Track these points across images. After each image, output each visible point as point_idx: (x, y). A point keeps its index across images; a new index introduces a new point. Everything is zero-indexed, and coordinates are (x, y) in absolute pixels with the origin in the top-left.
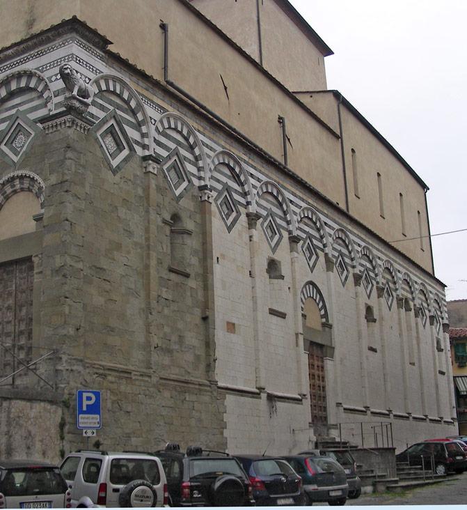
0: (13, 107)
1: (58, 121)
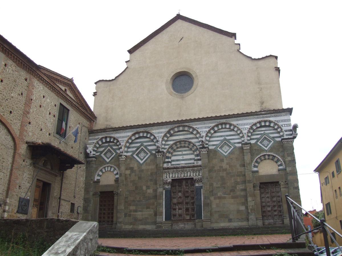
1: (290, 140)
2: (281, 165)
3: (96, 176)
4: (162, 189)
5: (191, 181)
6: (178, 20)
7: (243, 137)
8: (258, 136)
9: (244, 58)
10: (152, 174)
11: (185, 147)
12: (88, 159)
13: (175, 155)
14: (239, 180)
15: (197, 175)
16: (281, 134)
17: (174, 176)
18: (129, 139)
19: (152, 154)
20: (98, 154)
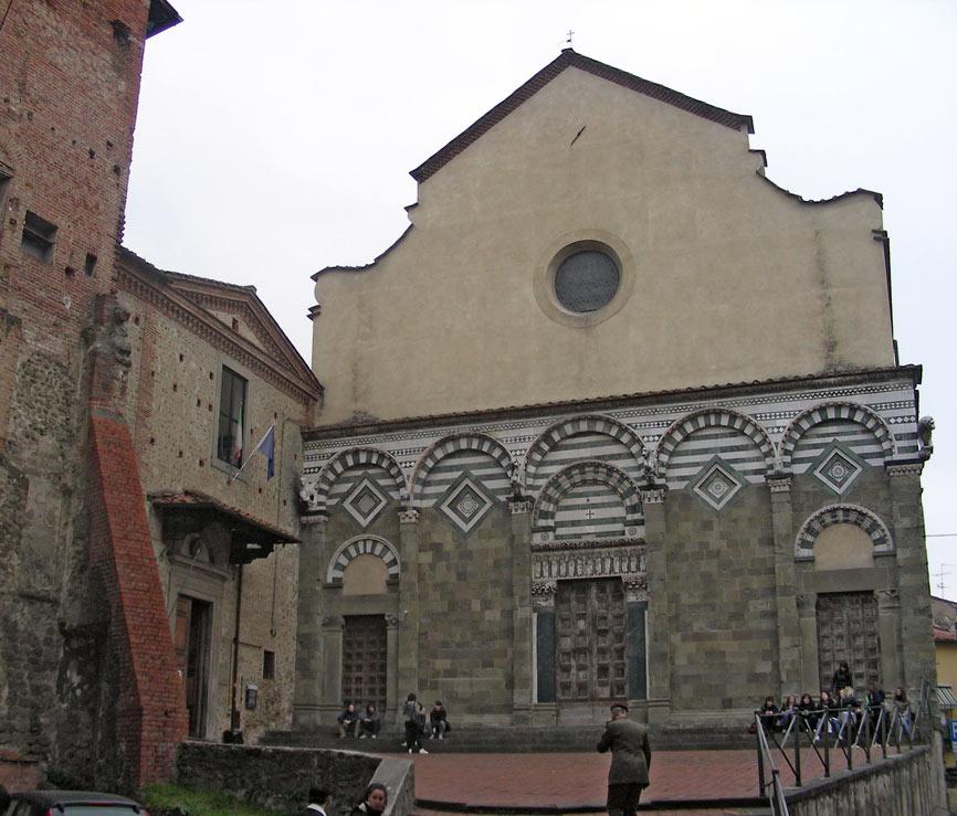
0: (828, 435)
1: (909, 466)
2: (882, 541)
3: (331, 568)
4: (528, 609)
5: (616, 585)
6: (566, 67)
7: (769, 454)
8: (817, 452)
9: (776, 198)
10: (497, 564)
11: (595, 482)
12: (304, 519)
13: (568, 508)
14: (755, 586)
15: (633, 568)
16: (886, 445)
18: (425, 458)
19: (496, 503)
20: (333, 502)
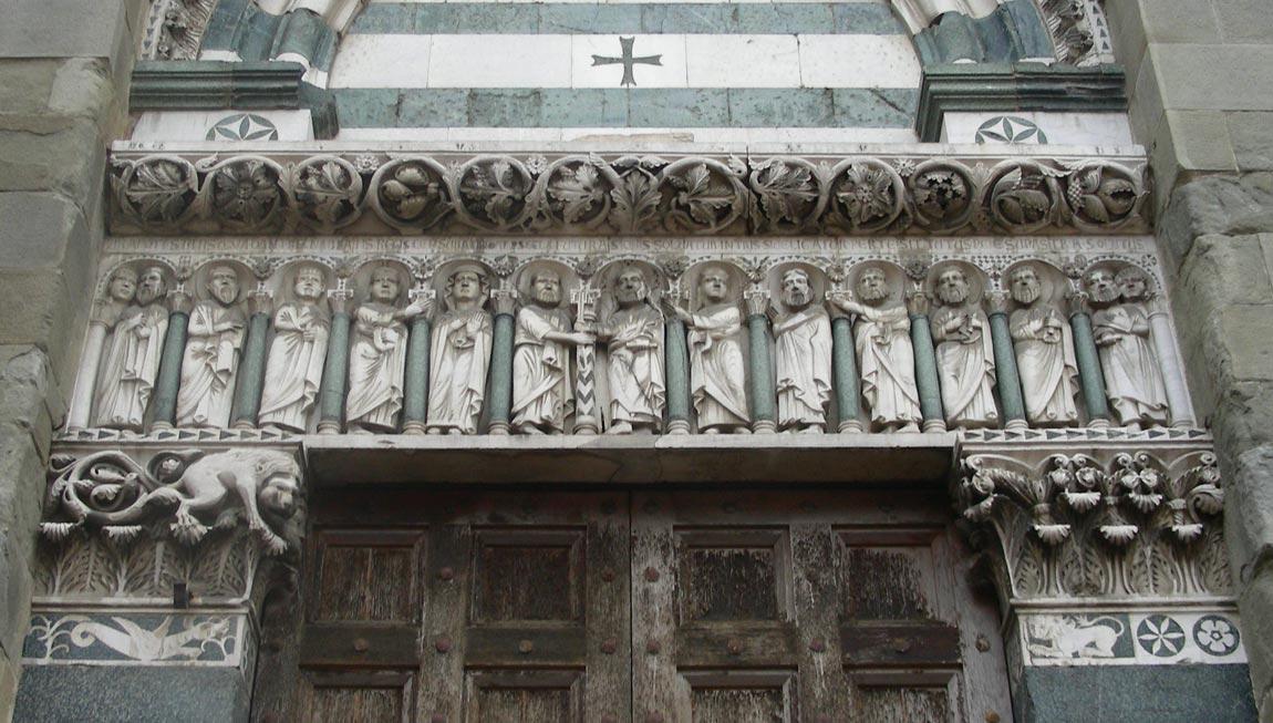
17: (390, 376)
